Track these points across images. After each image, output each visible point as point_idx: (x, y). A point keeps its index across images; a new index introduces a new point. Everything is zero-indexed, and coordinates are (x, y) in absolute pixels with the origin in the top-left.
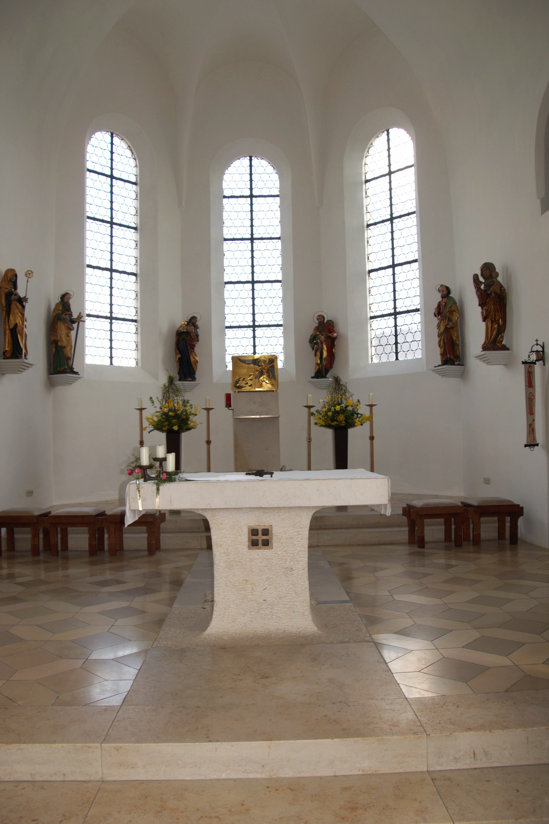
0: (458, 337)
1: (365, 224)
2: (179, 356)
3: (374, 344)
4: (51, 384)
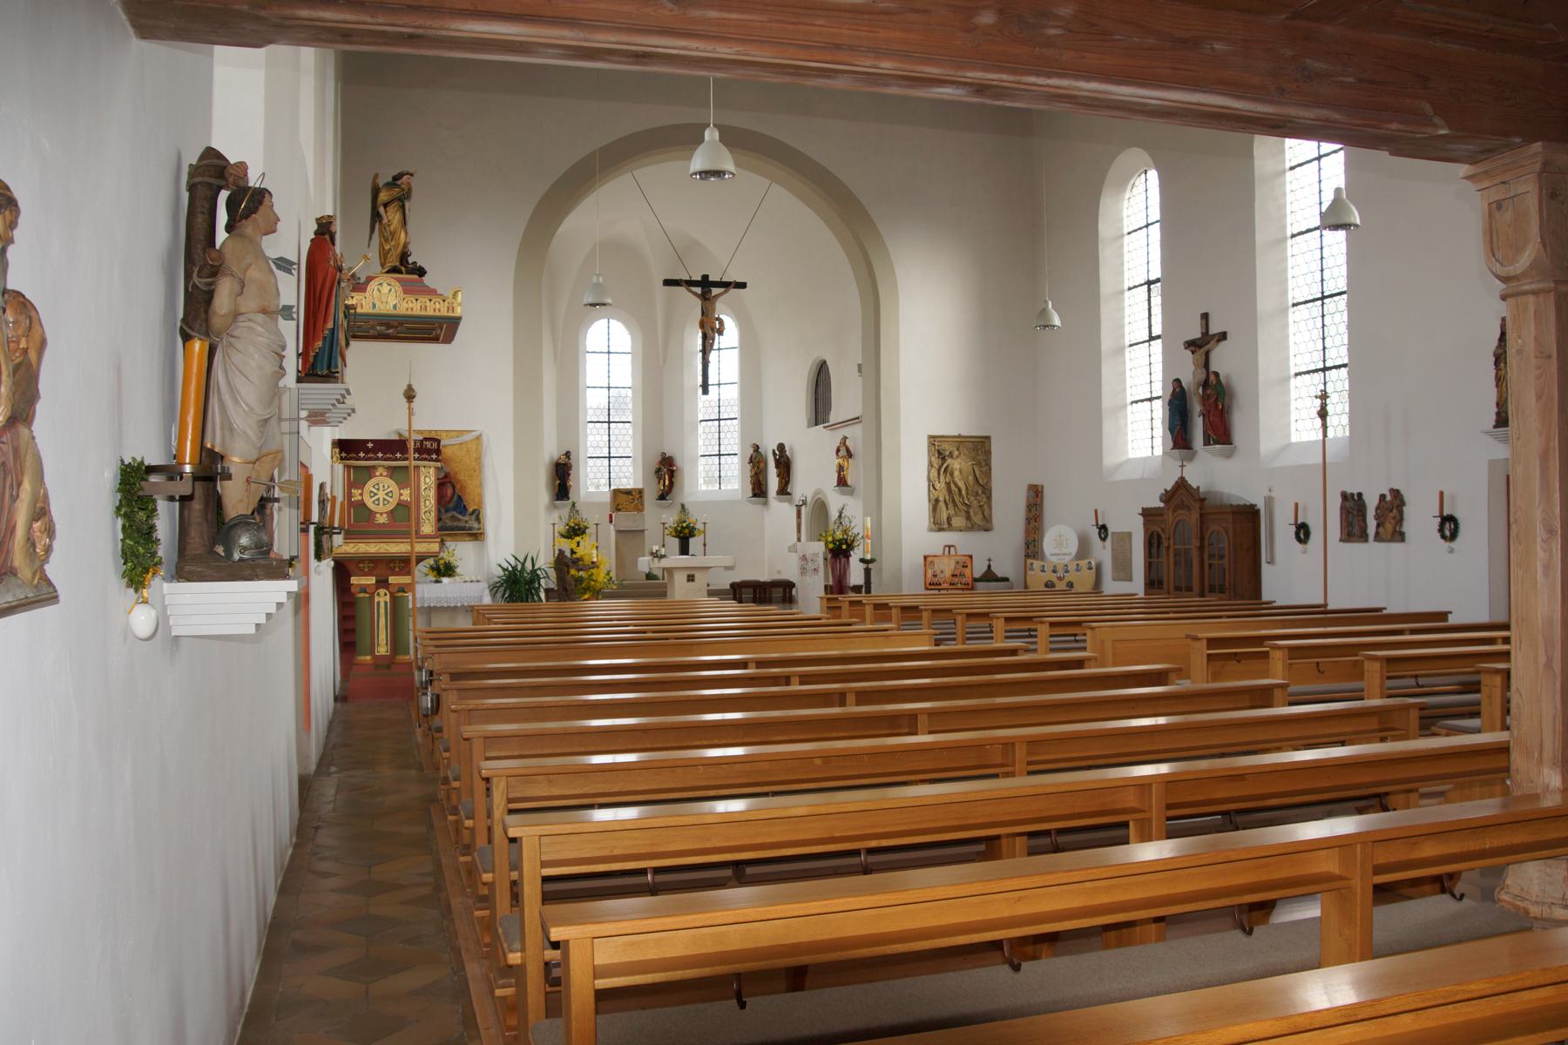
2: (558, 482)
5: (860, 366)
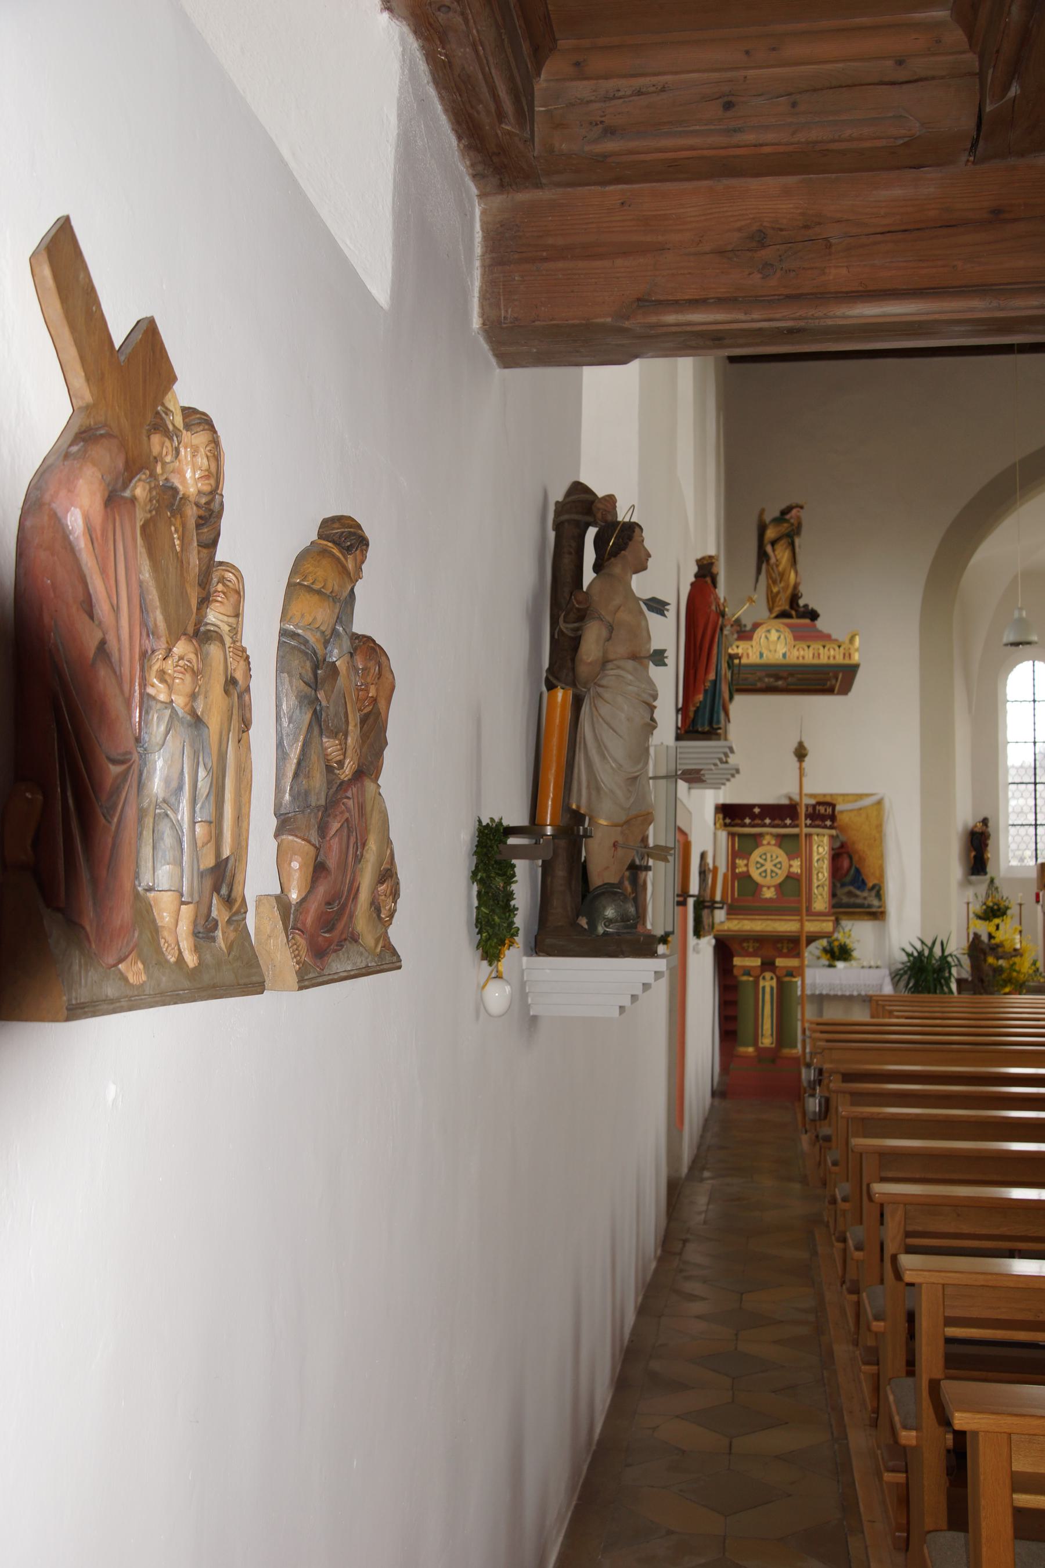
2: (973, 854)
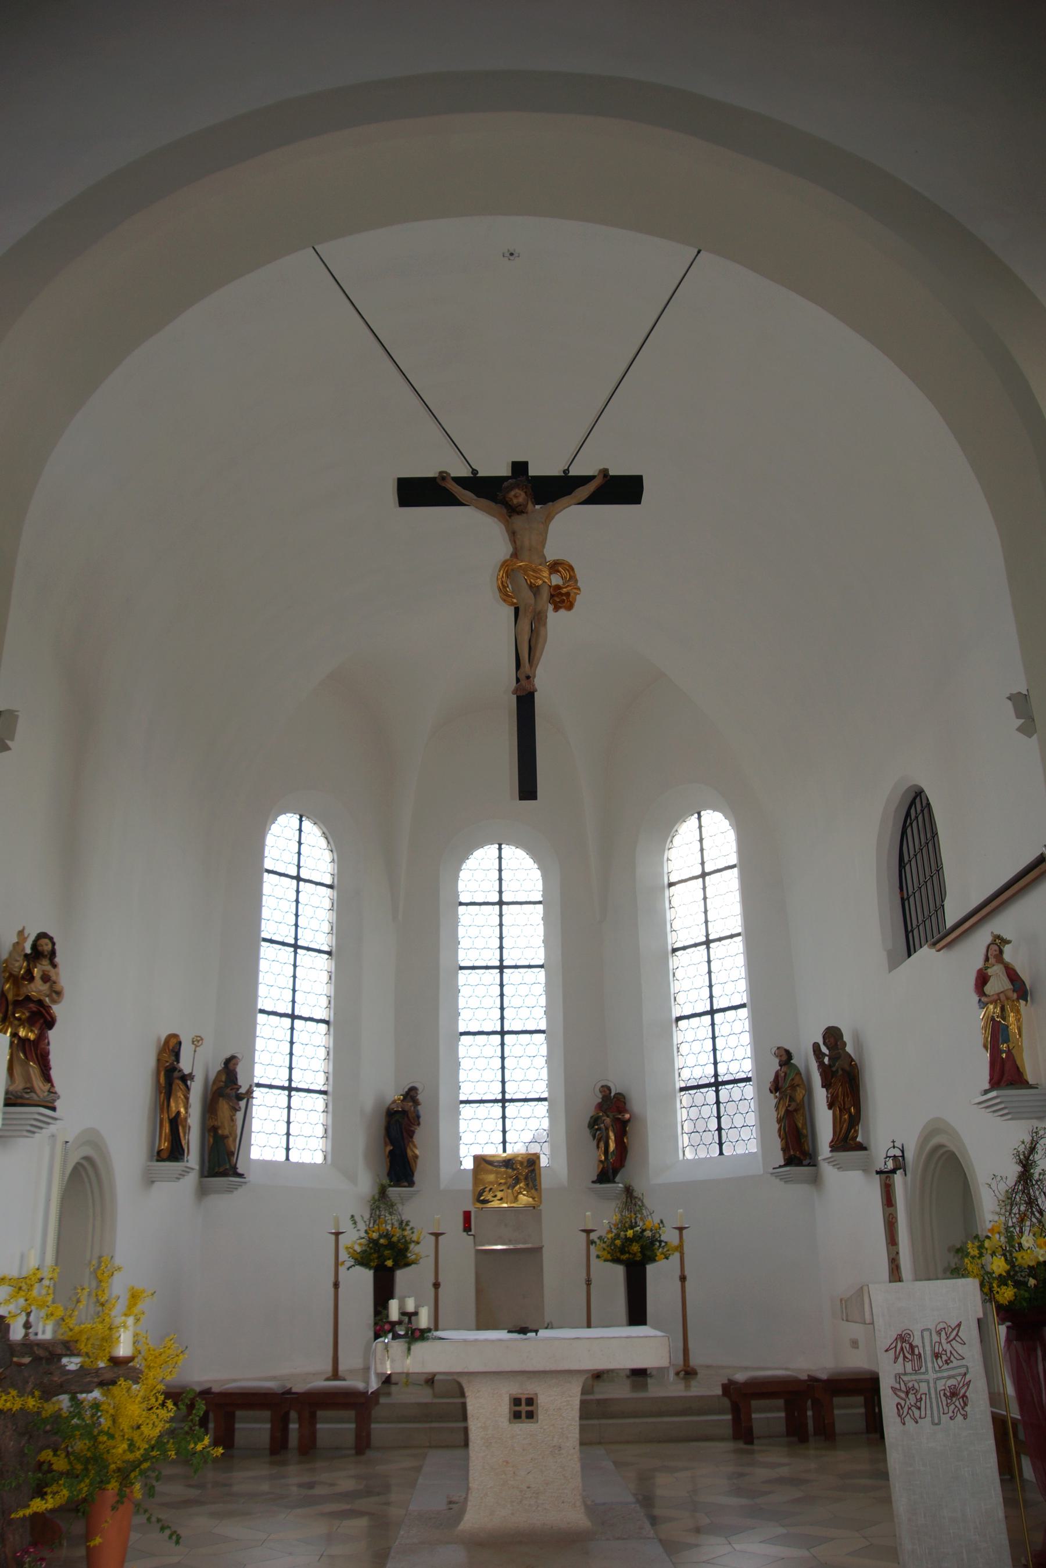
0: (805, 1124)
1: (670, 948)
2: (390, 1148)
3: (686, 1129)
4: (202, 1192)
5: (1021, 703)
